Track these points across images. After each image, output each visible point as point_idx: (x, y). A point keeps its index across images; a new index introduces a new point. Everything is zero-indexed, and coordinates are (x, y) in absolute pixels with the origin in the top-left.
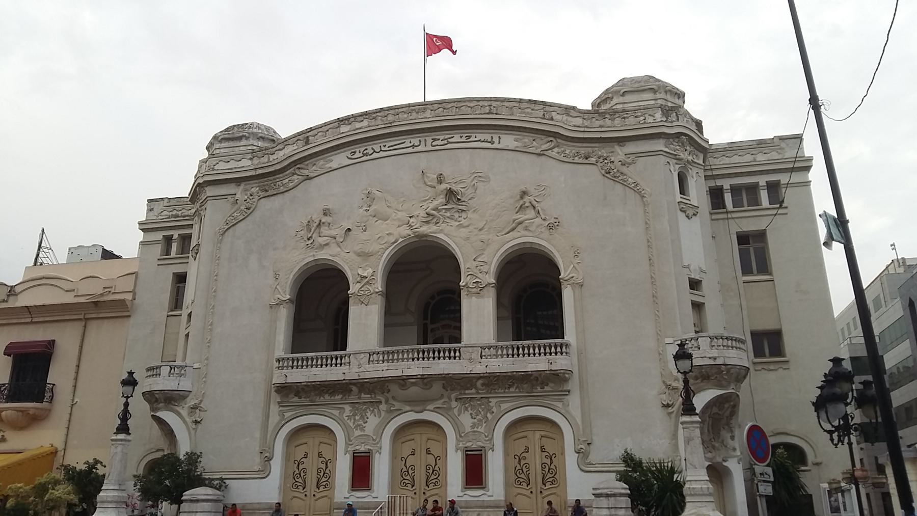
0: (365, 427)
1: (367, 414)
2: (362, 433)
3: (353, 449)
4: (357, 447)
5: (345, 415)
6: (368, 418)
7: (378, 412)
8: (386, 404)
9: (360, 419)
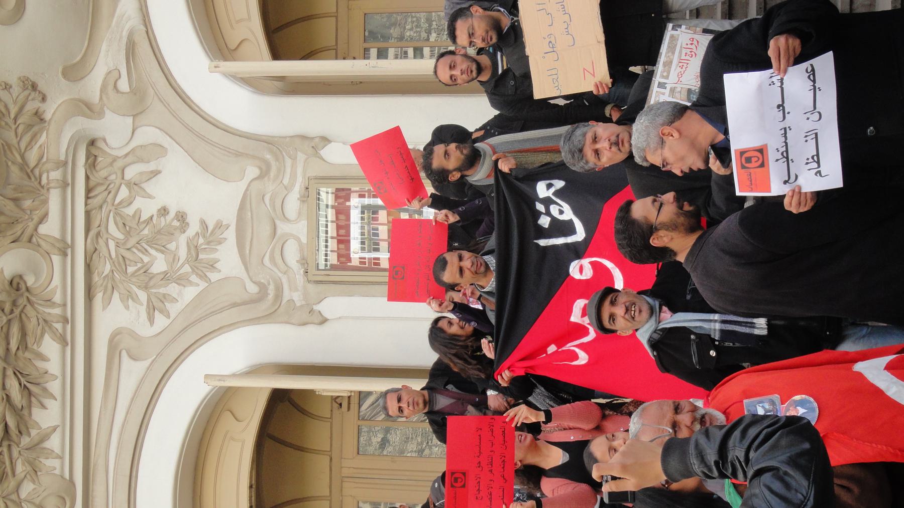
0: (203, 223)
1: (145, 216)
2: (231, 235)
3: (300, 279)
4: (292, 254)
5: (146, 330)
6: (164, 211)
7: (141, 160)
8: (100, 115)
9: (163, 250)
